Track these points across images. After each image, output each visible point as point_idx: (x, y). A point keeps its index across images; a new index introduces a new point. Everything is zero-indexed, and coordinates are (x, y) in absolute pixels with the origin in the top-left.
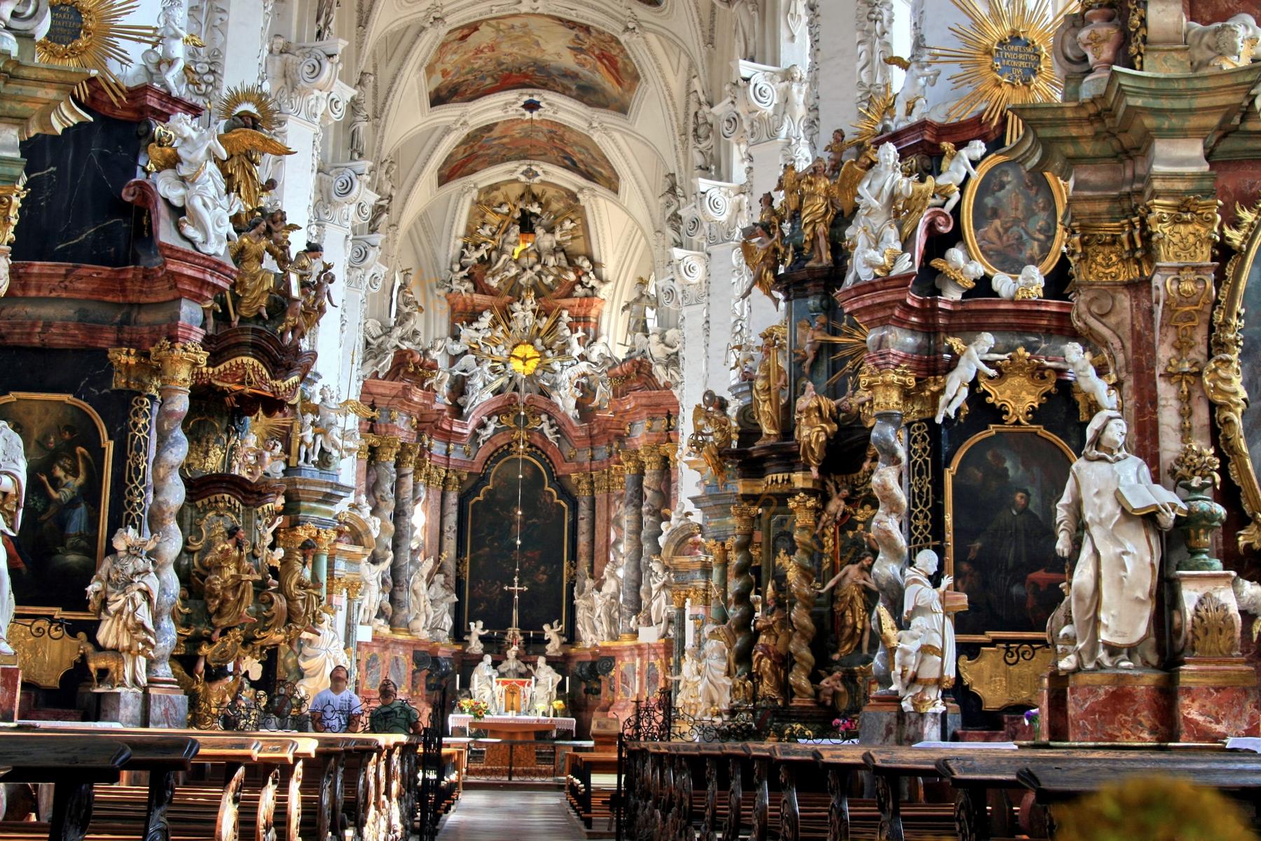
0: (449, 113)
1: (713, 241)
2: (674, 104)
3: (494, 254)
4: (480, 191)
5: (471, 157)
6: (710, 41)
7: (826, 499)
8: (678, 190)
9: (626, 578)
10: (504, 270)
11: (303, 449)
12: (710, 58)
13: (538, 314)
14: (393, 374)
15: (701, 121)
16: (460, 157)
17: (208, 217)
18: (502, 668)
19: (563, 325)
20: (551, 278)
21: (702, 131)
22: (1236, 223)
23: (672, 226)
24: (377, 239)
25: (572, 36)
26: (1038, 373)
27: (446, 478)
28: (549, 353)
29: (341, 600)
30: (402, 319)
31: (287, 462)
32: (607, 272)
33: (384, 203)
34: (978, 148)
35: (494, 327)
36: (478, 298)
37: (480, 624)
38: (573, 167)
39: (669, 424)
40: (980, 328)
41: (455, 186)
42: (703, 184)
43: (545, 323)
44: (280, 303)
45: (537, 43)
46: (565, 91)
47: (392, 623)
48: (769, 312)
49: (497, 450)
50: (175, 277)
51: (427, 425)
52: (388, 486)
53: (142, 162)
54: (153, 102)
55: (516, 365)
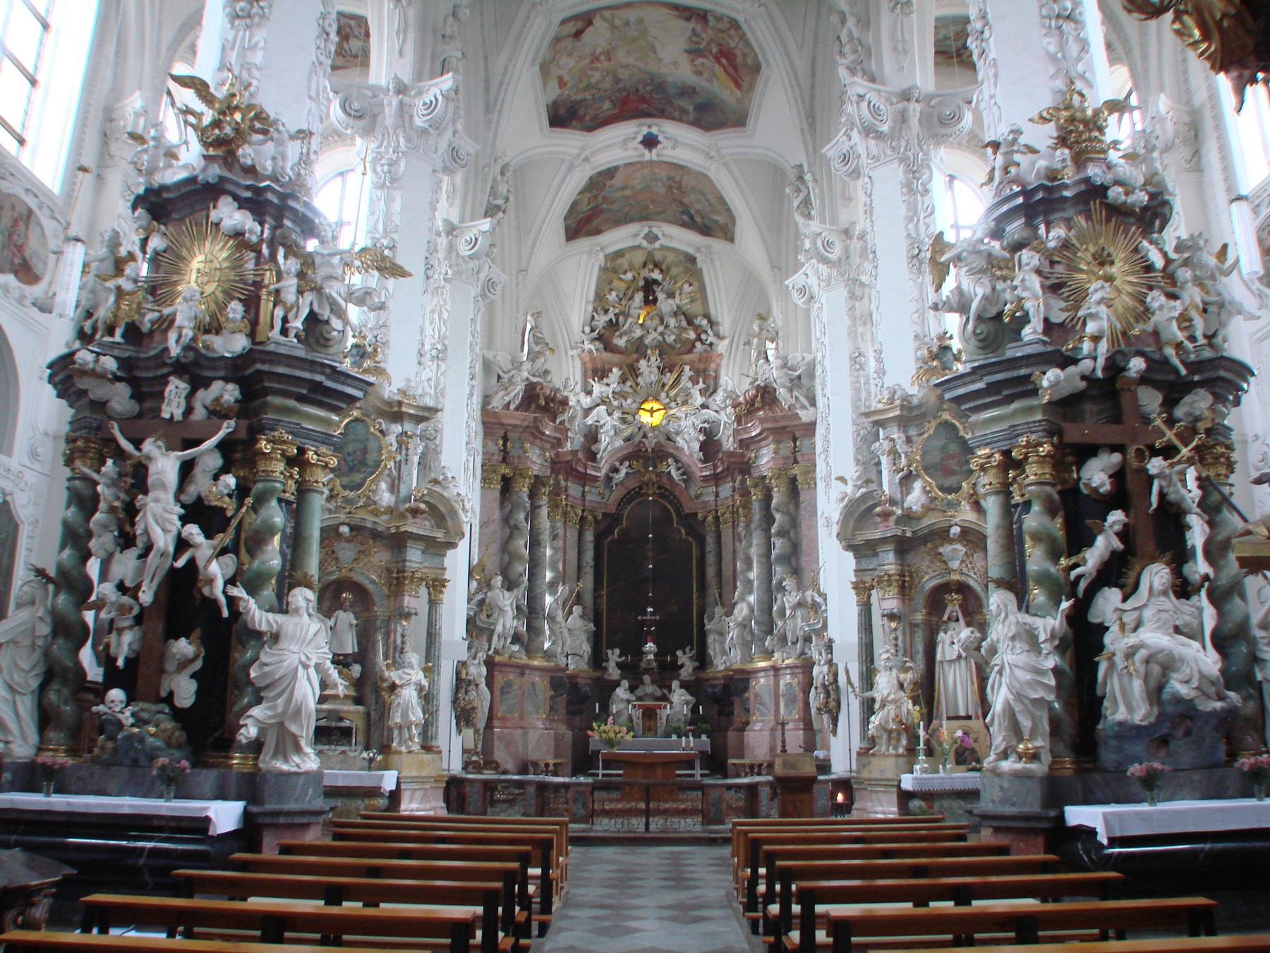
0: (570, 141)
2: (798, 84)
3: (621, 318)
4: (606, 256)
5: (595, 212)
8: (808, 177)
9: (759, 601)
10: (630, 331)
11: (279, 312)
13: (662, 371)
15: (844, 39)
16: (585, 207)
18: (639, 692)
19: (685, 378)
20: (673, 337)
21: (847, 49)
23: (802, 214)
25: (689, 33)
27: (583, 519)
28: (673, 404)
29: (416, 601)
30: (533, 356)
31: (252, 335)
32: (724, 329)
33: (500, 202)
35: (624, 383)
36: (607, 356)
37: (617, 651)
39: (795, 447)
41: (583, 244)
42: (858, 85)
43: (669, 378)
45: (655, 52)
46: (680, 117)
47: (529, 651)
49: (629, 493)
52: (522, 516)
55: (644, 417)
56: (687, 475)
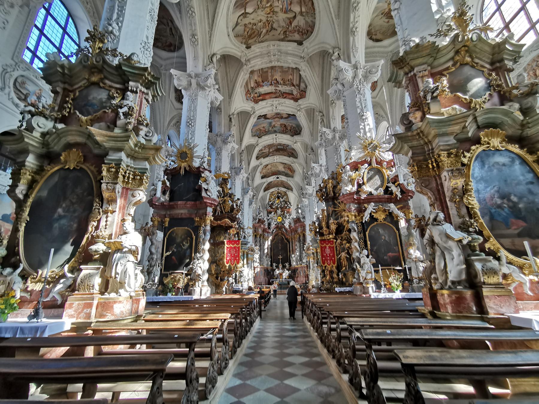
1: (309, 196)
6: (306, 163)
7: (337, 240)
12: (307, 166)
14: (258, 223)
17: (212, 191)
22: (465, 157)
24: (254, 200)
26: (385, 211)
34: (366, 165)
38: (285, 188)
40: (370, 202)
41: (266, 192)
42: (307, 187)
44: (232, 209)
46: (283, 175)
48: (323, 205)
50: (206, 203)
51: (264, 230)
53: (200, 181)
54: (201, 170)
55: (278, 220)
56: (286, 230)
